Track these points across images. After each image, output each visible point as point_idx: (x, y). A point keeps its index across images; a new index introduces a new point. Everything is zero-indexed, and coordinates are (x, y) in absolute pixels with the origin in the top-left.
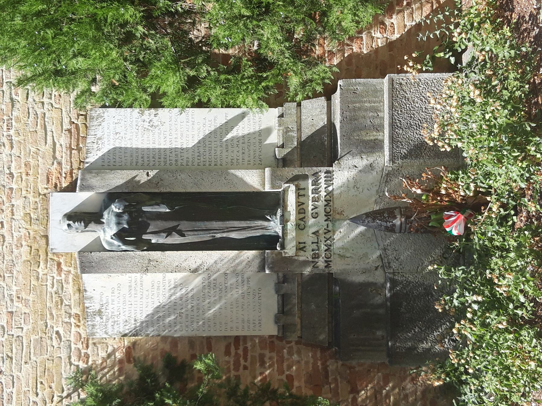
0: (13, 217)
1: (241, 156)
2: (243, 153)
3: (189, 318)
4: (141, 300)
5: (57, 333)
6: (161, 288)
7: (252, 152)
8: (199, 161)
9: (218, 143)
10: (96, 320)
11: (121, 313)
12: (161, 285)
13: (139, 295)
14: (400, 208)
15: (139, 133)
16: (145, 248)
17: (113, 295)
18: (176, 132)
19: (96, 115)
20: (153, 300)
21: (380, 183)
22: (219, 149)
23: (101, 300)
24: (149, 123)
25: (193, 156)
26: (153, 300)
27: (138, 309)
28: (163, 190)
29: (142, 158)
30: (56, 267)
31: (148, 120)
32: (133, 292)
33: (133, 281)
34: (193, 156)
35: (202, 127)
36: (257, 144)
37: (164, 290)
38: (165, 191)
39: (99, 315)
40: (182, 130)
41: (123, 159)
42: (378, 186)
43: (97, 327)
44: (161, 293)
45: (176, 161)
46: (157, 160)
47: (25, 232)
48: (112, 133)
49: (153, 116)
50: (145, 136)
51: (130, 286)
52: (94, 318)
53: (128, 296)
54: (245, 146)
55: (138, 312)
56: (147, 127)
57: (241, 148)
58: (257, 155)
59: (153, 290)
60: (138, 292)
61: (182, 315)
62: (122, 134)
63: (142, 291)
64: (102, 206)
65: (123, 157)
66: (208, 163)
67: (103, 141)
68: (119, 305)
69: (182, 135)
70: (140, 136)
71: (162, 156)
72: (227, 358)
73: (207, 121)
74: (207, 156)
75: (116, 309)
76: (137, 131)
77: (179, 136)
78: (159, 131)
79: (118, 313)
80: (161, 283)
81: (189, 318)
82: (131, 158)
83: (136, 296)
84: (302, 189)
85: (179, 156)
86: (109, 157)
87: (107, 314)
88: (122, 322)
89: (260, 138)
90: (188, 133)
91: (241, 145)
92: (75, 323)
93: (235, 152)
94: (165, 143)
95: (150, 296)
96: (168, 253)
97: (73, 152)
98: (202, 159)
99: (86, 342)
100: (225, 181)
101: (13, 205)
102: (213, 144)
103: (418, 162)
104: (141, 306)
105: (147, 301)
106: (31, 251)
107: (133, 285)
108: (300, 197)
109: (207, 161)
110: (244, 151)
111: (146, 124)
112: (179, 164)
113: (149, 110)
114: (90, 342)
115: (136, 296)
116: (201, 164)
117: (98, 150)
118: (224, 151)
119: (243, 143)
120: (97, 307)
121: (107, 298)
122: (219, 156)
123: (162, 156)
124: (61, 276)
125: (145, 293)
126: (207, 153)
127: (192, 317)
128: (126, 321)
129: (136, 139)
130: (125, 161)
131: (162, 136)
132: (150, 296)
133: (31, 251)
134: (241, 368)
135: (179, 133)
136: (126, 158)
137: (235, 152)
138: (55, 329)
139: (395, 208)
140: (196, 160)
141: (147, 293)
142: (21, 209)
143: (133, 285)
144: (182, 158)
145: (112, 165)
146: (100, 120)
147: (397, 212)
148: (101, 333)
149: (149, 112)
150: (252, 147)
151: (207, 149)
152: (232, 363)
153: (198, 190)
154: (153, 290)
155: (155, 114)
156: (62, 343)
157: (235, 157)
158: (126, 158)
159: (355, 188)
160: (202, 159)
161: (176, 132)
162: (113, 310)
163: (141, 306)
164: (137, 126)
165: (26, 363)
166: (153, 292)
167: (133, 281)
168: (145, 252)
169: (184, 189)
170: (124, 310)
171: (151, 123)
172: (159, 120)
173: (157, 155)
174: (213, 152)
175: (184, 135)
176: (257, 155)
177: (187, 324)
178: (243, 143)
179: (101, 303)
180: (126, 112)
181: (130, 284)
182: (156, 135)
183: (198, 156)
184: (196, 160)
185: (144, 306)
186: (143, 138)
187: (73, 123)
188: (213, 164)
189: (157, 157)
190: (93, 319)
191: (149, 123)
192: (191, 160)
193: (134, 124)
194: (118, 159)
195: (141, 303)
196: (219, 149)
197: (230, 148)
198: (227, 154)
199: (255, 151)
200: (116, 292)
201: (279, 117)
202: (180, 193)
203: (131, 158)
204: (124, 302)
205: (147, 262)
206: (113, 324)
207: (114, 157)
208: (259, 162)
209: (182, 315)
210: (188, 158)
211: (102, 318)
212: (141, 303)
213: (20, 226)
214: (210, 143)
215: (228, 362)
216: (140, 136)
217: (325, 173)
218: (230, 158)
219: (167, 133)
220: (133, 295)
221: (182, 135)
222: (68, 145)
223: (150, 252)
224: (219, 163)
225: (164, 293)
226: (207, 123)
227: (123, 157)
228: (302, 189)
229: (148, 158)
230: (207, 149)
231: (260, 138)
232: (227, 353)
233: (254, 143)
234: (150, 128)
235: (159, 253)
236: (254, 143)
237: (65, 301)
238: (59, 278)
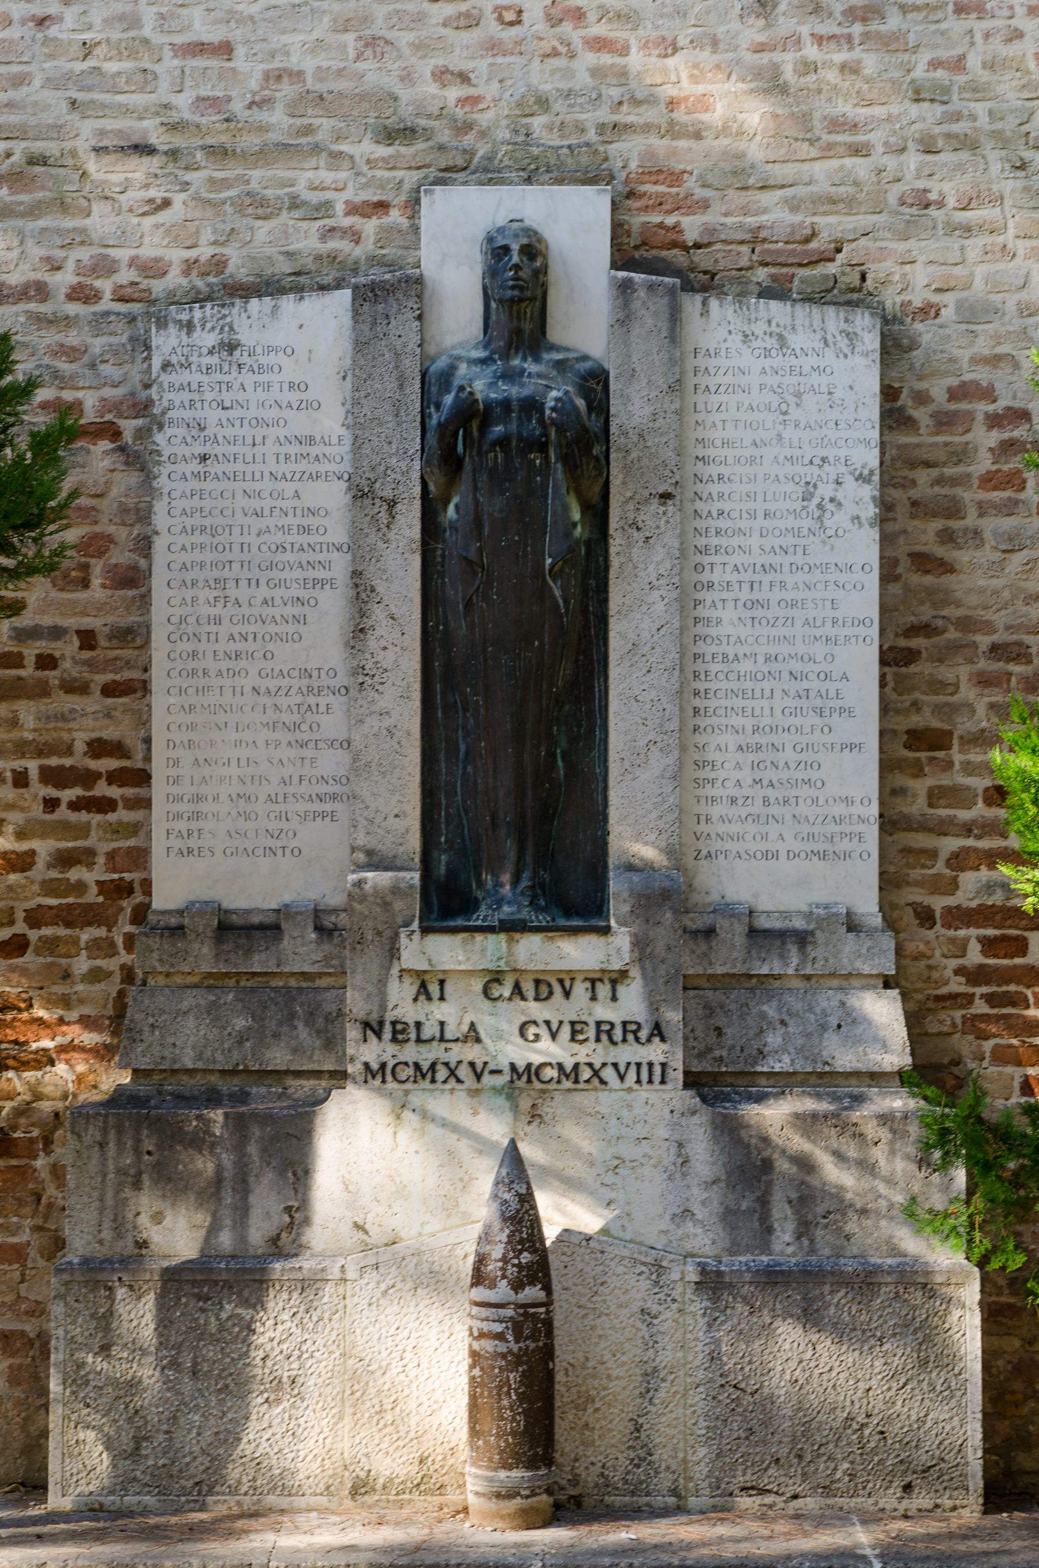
0: (537, 60)
1: (724, 793)
2: (733, 801)
3: (208, 628)
4: (267, 475)
5: (166, 203)
6: (304, 539)
7: (734, 828)
8: (708, 658)
9: (766, 721)
10: (205, 334)
11: (230, 414)
12: (313, 539)
13: (283, 468)
14: (548, 1304)
15: (799, 469)
16: (432, 487)
17: (286, 387)
18: (801, 586)
19: (858, 330)
20: (267, 512)
21: (631, 1241)
22: (748, 723)
23: (270, 349)
24: (832, 500)
25: (724, 640)
26: (267, 512)
27: (239, 467)
28: (615, 545)
29: (720, 478)
30: (375, 199)
31: (840, 496)
32: (293, 449)
33: (328, 450)
34: (724, 640)
35: (817, 668)
36: (764, 846)
37: (297, 547)
38: (613, 550)
39: (222, 344)
40: (810, 604)
41: (717, 417)
42: (621, 1235)
43: (184, 337)
44: (289, 539)
45: (710, 586)
46: (713, 524)
47: (489, 98)
48: (801, 379)
49: (855, 510)
50: (790, 487)
51: (311, 440)
52: (213, 328)
53: (281, 432)
54: (758, 808)
55: (230, 468)
56: (819, 492)
57: (749, 792)
58: (729, 845)
59: (299, 512)
60: (293, 467)
61: (220, 605)
62: (795, 414)
63: (297, 476)
64: (567, 349)
65: (723, 416)
66: (701, 686)
67: (774, 353)
68: (253, 405)
69: (793, 604)
70: (789, 469)
71: (723, 541)
72: (80, 747)
73: (838, 685)
74: (724, 685)
75: (241, 396)
76: (806, 461)
77: (789, 595)
78: (805, 531)
79: (227, 404)
80: (321, 539)
81: (208, 628)
82: (718, 443)
83: (282, 458)
84: (614, 991)
85: (725, 595)
86: (722, 371)
87: (226, 368)
88: (199, 414)
89: (783, 855)
90: (798, 623)
91: (759, 793)
92: (196, 261)
93: (736, 775)
94: (768, 549)
95: (279, 503)
96: (416, 562)
97: (745, 249)
98: (714, 668)
99: (136, 295)
100: (643, 742)
101: (572, 56)
102: (765, 703)
103: (697, 1363)
104: (249, 477)
105: (265, 494)
106: (429, 116)
107: (315, 451)
108: (588, 985)
109: (707, 685)
110: (740, 802)
111: (826, 490)
112: (700, 596)
113: (874, 498)
114: (136, 308)
115: (282, 458)
116: (700, 667)
117: (746, 336)
118: (741, 739)
119: (766, 801)
120: (245, 336)
121: (276, 369)
122: (724, 721)
123: (723, 541)
124: (347, 214)
125: (289, 488)
126: (734, 685)
127: (213, 637)
128: (203, 429)
129: (781, 459)
130: (708, 424)
131: (789, 541)
132: (279, 503)
133: (429, 116)
134: (52, 792)
135: (798, 595)
136: (720, 425)
137: (736, 775)
138: (178, 199)
139: (548, 1288)
140: (713, 649)
141: (289, 493)
142: (564, 85)
143: (315, 451)
144: (719, 605)
145: (695, 381)
146: (843, 343)
147: (533, 1293)
148: (166, 349)
149: (867, 499)
150: (751, 828)
151: (748, 685)
152: (68, 762)
153: (613, 656)
154: (299, 512)
155: (858, 518)
156: (135, 220)
157: (722, 774)
158: (720, 425)
159: (616, 1162)
160: (714, 668)
161: (801, 586)
162: (236, 386)
163: (249, 477)
164: (824, 460)
165: (73, 103)
166: (291, 512)
167: (328, 450)
168: (418, 490)
169: (619, 612)
170: (238, 423)
171: (830, 506)
172: (840, 532)
173: (729, 523)
174: (738, 703)
175: (790, 612)
176: (729, 845)
177: (191, 620)
178: (766, 801)
179: (259, 350)
180: (869, 425)
181: (318, 439)
182: (790, 522)
183: (725, 656)
184: (713, 649)
185: (249, 486)
186: (782, 478)
187: (839, 250)
188: (697, 702)
189: (722, 524)
190: (209, 326)
191: (832, 500)
192: (713, 631)
193: (830, 453)
194: (715, 399)
195: (258, 476)
196: (748, 723)
197: (751, 757)
198: (732, 747)
199: (739, 838)
200: (294, 397)
201: (849, 914)
202: (606, 600)
203: (718, 443)
204: (260, 422)
205: (388, 493)
206: (194, 386)
207: (722, 389)
208: (704, 853)
209: (220, 605)
210: (719, 622)
211: (210, 352)
212: (258, 476)
213: (509, 83)
214: (767, 693)
215: (69, 751)
216: (789, 469)
217: (664, 1065)
218: (718, 757)
219: (799, 559)
220: (282, 450)
221: (793, 604)
222: (763, 234)
223: (417, 503)
224: (702, 722)
225: (289, 547)
226: (832, 687)
227: (723, 416)
228: (614, 991)
229: (721, 496)
230: (748, 685)
231: (783, 855)
232: (98, 748)
233: (765, 837)
234: (816, 501)
235: (416, 532)
236: (765, 837)
237: (268, 225)
238: (340, 208)
